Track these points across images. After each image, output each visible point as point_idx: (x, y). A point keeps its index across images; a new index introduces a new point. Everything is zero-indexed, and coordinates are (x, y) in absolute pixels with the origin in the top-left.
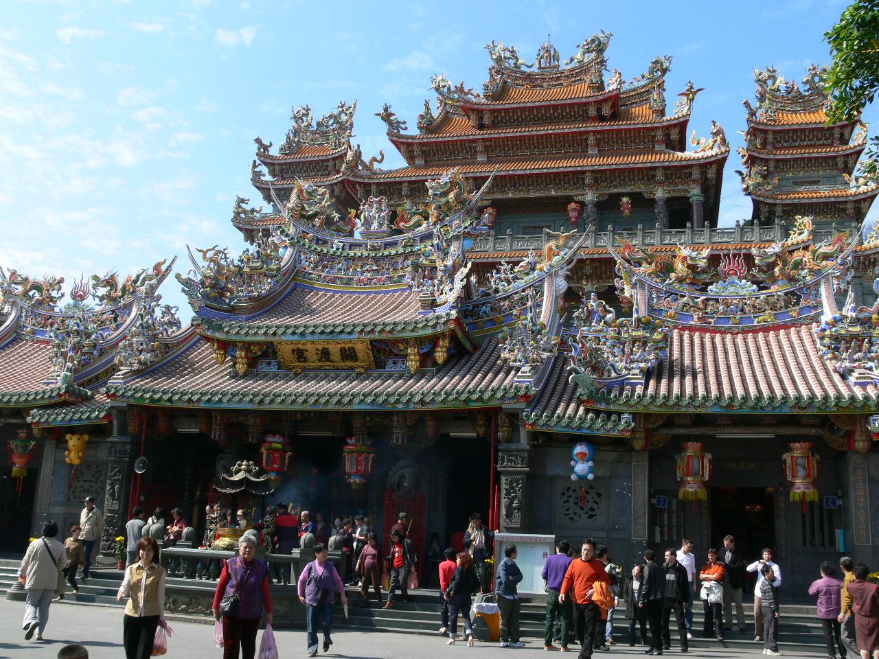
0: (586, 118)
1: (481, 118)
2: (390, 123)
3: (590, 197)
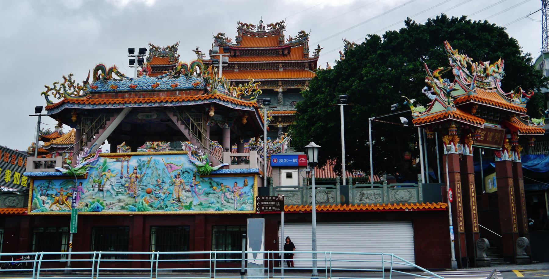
1: (235, 53)
2: (199, 55)
3: (280, 90)
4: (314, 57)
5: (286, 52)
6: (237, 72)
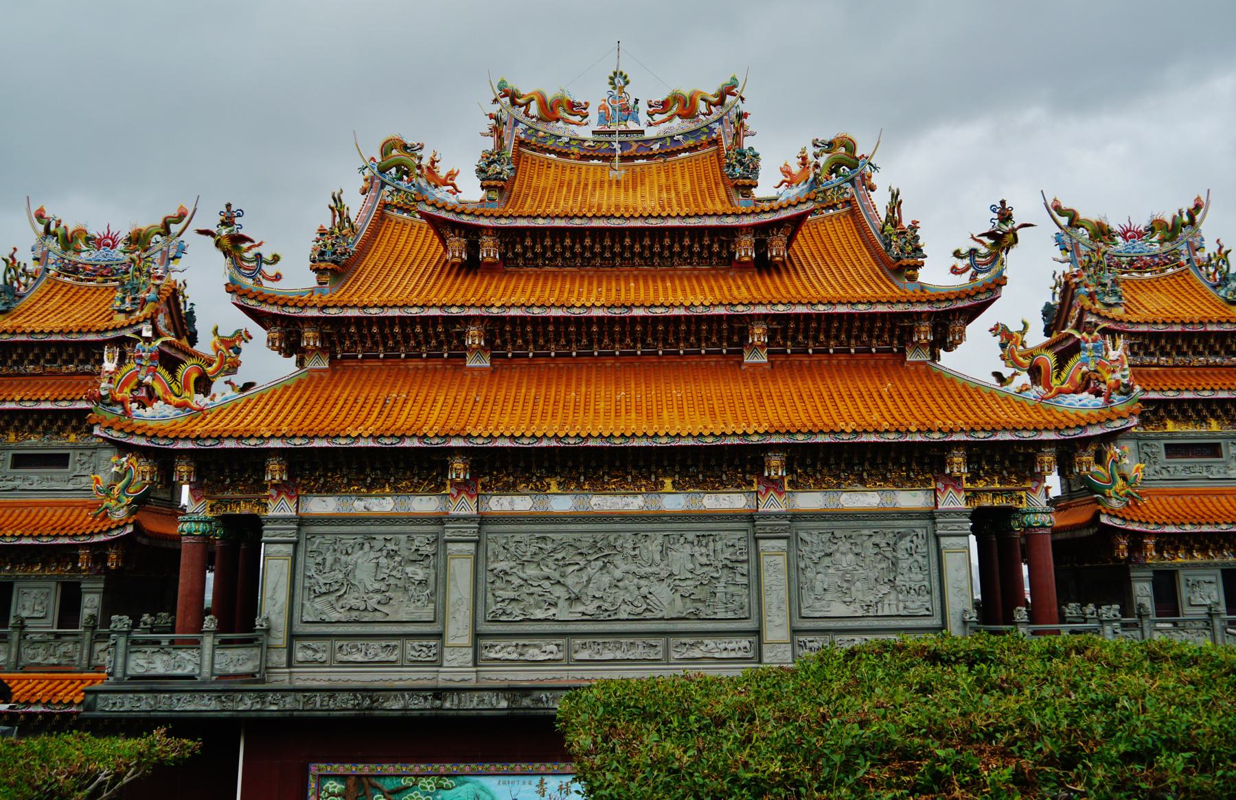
0: (727, 263)
1: (473, 248)
4: (964, 279)
5: (777, 250)
6: (481, 369)
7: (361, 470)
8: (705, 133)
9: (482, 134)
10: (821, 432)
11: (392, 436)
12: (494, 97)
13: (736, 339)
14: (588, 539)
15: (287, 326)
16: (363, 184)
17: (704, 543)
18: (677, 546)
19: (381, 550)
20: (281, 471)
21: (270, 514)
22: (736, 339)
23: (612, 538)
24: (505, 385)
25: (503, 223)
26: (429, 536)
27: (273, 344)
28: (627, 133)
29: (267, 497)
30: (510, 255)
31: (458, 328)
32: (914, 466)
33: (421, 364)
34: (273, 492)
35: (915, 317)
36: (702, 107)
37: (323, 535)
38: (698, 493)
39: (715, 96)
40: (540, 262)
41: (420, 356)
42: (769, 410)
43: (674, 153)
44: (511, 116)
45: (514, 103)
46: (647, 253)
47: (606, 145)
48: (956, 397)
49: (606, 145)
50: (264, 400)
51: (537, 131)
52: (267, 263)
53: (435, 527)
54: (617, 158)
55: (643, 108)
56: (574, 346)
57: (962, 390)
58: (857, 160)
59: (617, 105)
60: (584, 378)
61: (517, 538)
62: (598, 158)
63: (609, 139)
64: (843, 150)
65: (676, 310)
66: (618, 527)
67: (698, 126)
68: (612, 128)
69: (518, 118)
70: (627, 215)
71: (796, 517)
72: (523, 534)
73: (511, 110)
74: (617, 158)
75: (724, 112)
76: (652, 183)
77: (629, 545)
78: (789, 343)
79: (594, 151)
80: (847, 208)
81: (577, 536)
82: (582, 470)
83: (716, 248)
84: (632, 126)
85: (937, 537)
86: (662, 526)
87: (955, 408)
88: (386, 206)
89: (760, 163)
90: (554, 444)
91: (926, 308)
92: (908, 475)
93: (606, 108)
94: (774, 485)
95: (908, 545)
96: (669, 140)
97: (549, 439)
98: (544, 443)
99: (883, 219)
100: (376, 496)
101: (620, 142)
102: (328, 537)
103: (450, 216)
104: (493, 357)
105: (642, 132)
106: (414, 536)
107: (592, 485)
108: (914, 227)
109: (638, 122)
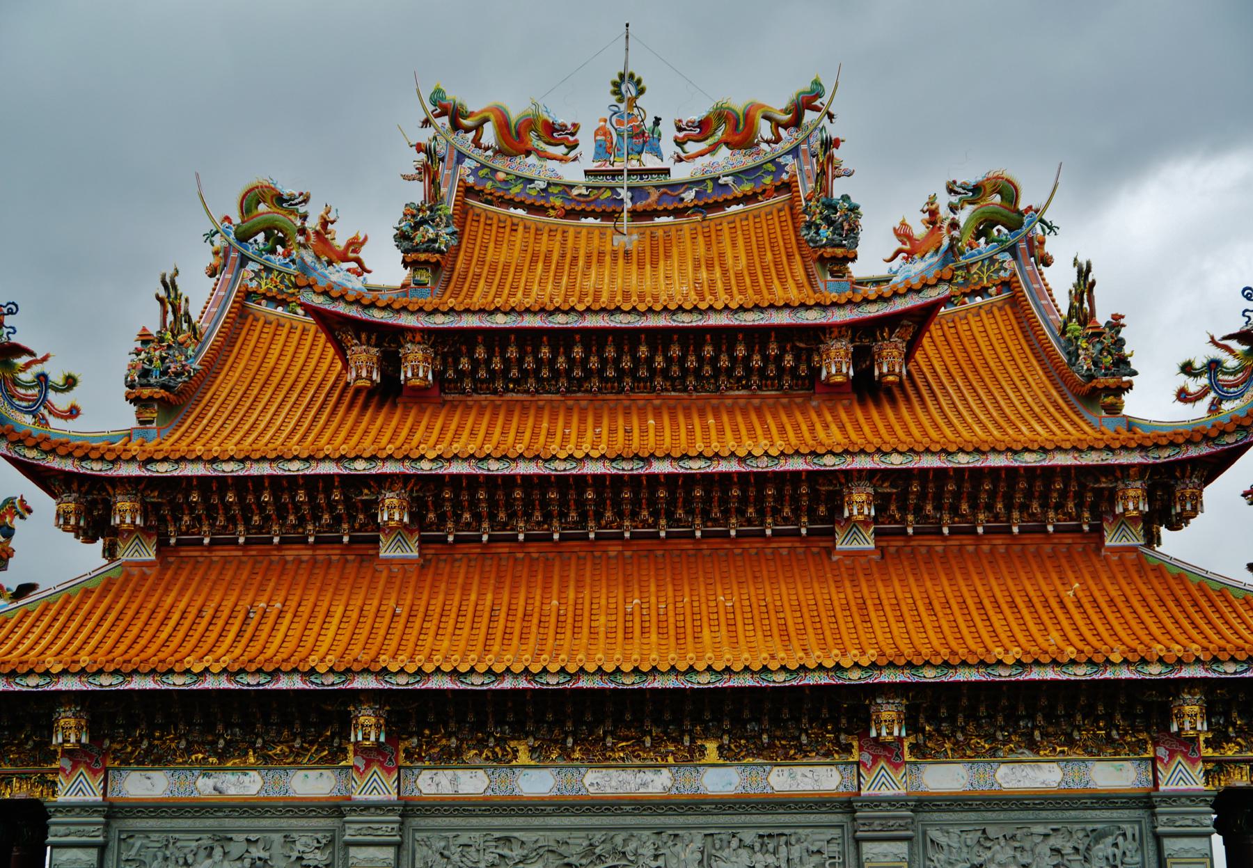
1: (390, 363)
5: (890, 364)
6: (404, 562)
7: (209, 727)
8: (768, 173)
9: (405, 177)
10: (964, 664)
11: (259, 671)
12: (424, 117)
13: (822, 510)
14: (579, 842)
15: (88, 492)
16: (211, 260)
17: (771, 847)
18: (726, 853)
19: (241, 858)
20: (79, 728)
21: (61, 798)
22: (822, 510)
23: (619, 840)
24: (443, 586)
25: (440, 321)
26: (319, 836)
27: (66, 522)
28: (641, 173)
29: (56, 772)
30: (450, 374)
31: (366, 495)
32: (1118, 719)
33: (306, 554)
34: (65, 763)
35: (1118, 474)
36: (765, 129)
37: (146, 833)
38: (761, 765)
39: (786, 111)
40: (499, 385)
41: (304, 540)
42: (876, 626)
43: (718, 206)
44: (452, 147)
45: (456, 126)
46: (675, 370)
47: (608, 194)
48: (1187, 604)
49: (608, 194)
50: (52, 613)
51: (494, 171)
52: (57, 390)
53: (329, 821)
54: (625, 214)
55: (668, 133)
56: (556, 523)
57: (1197, 594)
58: (1021, 214)
59: (625, 127)
60: (573, 575)
61: (464, 838)
62: (594, 214)
63: (612, 183)
64: (997, 199)
65: (723, 463)
66: (629, 820)
67: (759, 161)
68: (617, 166)
69: (464, 150)
70: (642, 308)
71: (923, 804)
72: (472, 832)
73: (452, 137)
74: (625, 214)
75: (801, 137)
76: (682, 254)
77: (648, 851)
78: (910, 518)
79: (588, 203)
80: (1005, 295)
81: (560, 835)
82: (569, 727)
83: (789, 360)
84: (650, 161)
85: (1158, 838)
86: (702, 820)
87: (1185, 623)
88: (248, 295)
89: (861, 221)
90: (523, 684)
91: (1136, 458)
92: (1108, 735)
93: (606, 133)
94: (887, 751)
95: (1110, 851)
96: (710, 184)
97: (516, 676)
98: (508, 684)
99: (1065, 311)
100: (234, 769)
101: (630, 189)
102: (154, 837)
103: (353, 312)
104: (423, 542)
105: (667, 172)
106: (295, 835)
107: (586, 752)
108: (1116, 324)
109: (659, 155)
